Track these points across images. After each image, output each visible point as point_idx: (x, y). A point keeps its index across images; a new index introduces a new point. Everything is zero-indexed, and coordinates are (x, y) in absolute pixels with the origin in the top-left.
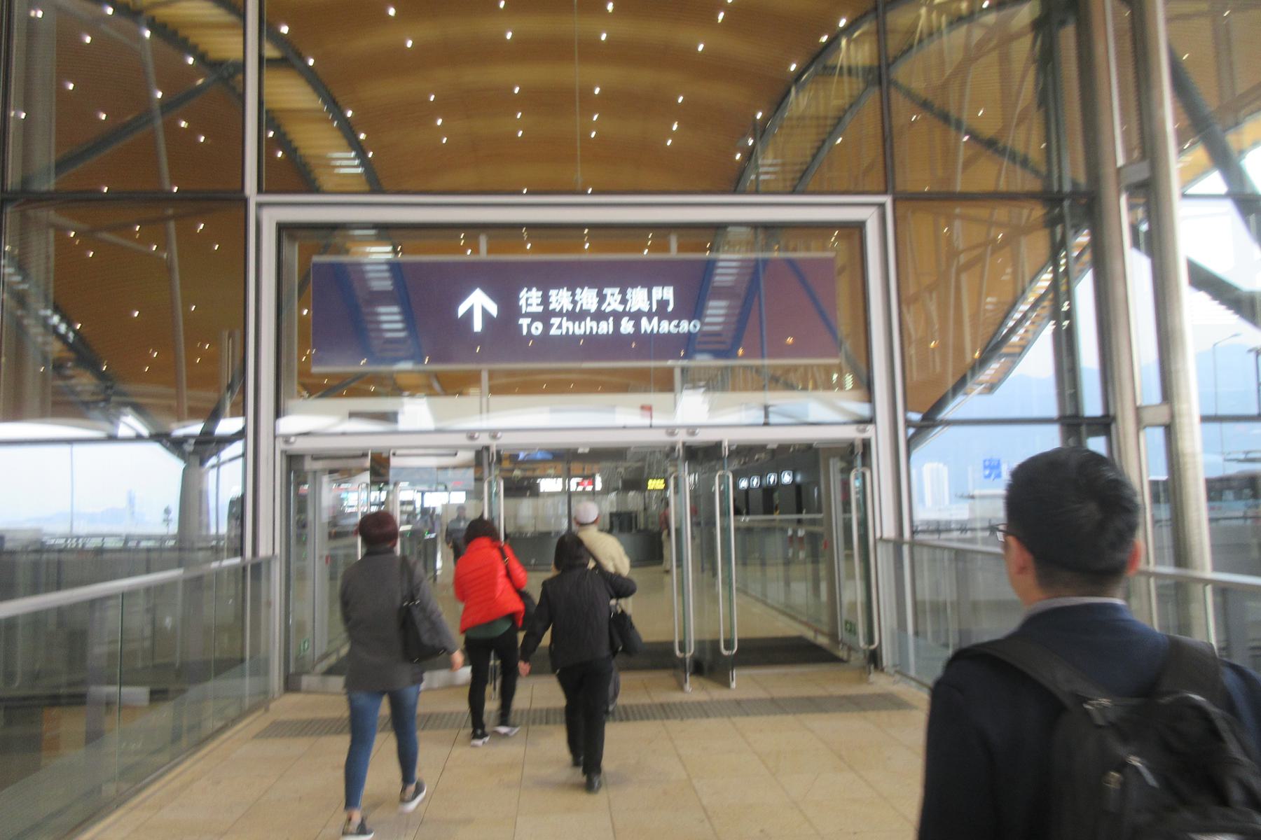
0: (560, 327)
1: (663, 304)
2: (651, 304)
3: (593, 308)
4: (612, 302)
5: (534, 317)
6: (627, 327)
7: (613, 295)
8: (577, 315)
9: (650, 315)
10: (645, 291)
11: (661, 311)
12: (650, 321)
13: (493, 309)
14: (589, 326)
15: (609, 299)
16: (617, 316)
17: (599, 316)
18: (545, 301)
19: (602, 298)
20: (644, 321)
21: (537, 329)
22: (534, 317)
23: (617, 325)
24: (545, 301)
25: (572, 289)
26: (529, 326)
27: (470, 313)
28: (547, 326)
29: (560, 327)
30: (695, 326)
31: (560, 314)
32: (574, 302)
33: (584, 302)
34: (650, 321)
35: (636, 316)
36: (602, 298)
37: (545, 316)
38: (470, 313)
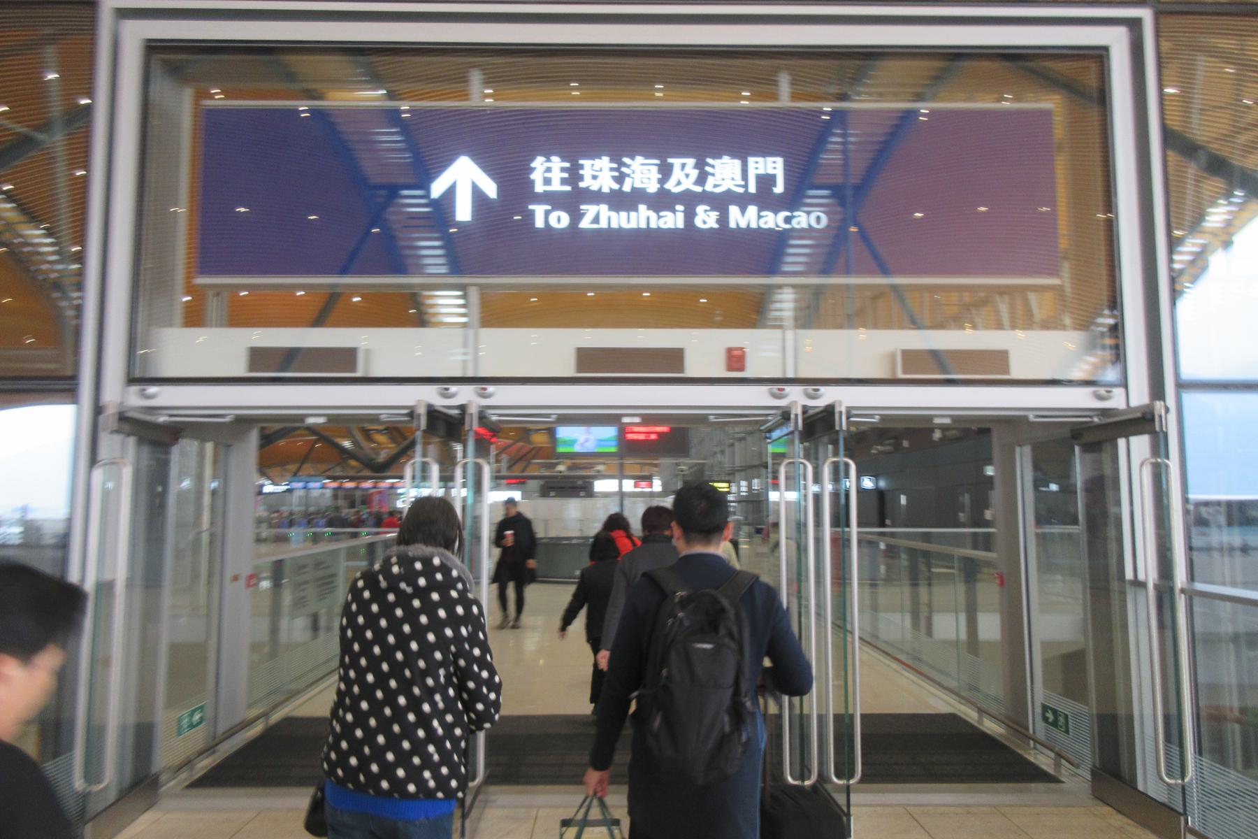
0: (596, 220)
1: (766, 181)
2: (746, 186)
3: (653, 188)
4: (683, 179)
5: (555, 201)
6: (706, 218)
7: (683, 166)
8: (621, 201)
9: (743, 201)
10: (737, 163)
11: (764, 197)
12: (743, 211)
13: (490, 189)
14: (641, 218)
15: (677, 174)
16: (690, 201)
17: (662, 201)
18: (574, 175)
19: (666, 171)
20: (734, 211)
21: (561, 220)
22: (555, 201)
23: (690, 215)
24: (574, 175)
25: (616, 158)
26: (547, 213)
27: (451, 192)
28: (576, 216)
29: (596, 220)
30: (818, 219)
31: (596, 197)
32: (620, 179)
33: (637, 176)
34: (743, 211)
35: (720, 202)
36: (666, 171)
37: (573, 200)
38: (451, 192)
